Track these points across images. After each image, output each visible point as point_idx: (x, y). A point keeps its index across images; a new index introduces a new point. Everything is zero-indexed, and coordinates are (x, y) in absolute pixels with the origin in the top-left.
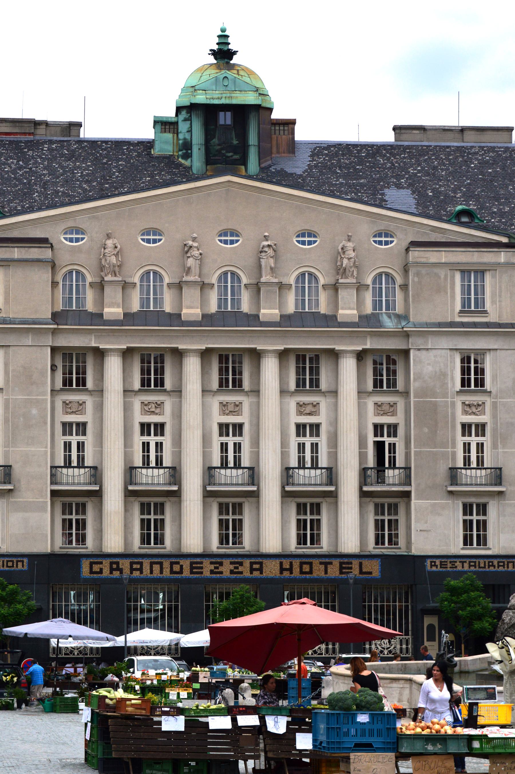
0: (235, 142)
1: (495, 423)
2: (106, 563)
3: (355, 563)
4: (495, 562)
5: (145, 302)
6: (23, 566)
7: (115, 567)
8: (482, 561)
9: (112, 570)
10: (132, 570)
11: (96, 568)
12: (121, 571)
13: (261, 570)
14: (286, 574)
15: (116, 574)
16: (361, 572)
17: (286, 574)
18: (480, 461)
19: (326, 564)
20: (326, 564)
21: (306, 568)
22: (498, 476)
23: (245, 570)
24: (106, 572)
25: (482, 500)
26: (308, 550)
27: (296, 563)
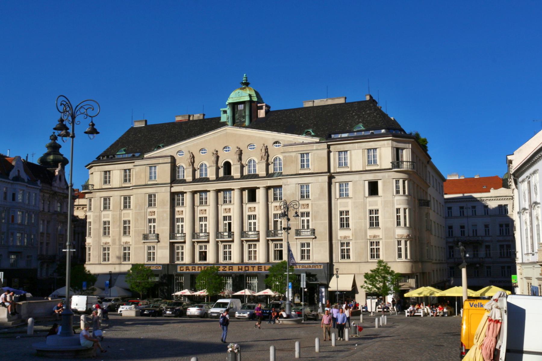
0: (243, 114)
1: (312, 211)
3: (263, 266)
4: (311, 266)
5: (201, 175)
7: (187, 269)
8: (306, 265)
9: (186, 269)
10: (192, 269)
11: (182, 269)
12: (189, 270)
13: (232, 269)
14: (240, 271)
15: (188, 271)
16: (265, 270)
17: (240, 271)
18: (308, 226)
19: (253, 267)
20: (253, 267)
21: (247, 268)
22: (313, 231)
23: (227, 269)
24: (185, 270)
25: (308, 241)
26: (252, 261)
27: (244, 266)
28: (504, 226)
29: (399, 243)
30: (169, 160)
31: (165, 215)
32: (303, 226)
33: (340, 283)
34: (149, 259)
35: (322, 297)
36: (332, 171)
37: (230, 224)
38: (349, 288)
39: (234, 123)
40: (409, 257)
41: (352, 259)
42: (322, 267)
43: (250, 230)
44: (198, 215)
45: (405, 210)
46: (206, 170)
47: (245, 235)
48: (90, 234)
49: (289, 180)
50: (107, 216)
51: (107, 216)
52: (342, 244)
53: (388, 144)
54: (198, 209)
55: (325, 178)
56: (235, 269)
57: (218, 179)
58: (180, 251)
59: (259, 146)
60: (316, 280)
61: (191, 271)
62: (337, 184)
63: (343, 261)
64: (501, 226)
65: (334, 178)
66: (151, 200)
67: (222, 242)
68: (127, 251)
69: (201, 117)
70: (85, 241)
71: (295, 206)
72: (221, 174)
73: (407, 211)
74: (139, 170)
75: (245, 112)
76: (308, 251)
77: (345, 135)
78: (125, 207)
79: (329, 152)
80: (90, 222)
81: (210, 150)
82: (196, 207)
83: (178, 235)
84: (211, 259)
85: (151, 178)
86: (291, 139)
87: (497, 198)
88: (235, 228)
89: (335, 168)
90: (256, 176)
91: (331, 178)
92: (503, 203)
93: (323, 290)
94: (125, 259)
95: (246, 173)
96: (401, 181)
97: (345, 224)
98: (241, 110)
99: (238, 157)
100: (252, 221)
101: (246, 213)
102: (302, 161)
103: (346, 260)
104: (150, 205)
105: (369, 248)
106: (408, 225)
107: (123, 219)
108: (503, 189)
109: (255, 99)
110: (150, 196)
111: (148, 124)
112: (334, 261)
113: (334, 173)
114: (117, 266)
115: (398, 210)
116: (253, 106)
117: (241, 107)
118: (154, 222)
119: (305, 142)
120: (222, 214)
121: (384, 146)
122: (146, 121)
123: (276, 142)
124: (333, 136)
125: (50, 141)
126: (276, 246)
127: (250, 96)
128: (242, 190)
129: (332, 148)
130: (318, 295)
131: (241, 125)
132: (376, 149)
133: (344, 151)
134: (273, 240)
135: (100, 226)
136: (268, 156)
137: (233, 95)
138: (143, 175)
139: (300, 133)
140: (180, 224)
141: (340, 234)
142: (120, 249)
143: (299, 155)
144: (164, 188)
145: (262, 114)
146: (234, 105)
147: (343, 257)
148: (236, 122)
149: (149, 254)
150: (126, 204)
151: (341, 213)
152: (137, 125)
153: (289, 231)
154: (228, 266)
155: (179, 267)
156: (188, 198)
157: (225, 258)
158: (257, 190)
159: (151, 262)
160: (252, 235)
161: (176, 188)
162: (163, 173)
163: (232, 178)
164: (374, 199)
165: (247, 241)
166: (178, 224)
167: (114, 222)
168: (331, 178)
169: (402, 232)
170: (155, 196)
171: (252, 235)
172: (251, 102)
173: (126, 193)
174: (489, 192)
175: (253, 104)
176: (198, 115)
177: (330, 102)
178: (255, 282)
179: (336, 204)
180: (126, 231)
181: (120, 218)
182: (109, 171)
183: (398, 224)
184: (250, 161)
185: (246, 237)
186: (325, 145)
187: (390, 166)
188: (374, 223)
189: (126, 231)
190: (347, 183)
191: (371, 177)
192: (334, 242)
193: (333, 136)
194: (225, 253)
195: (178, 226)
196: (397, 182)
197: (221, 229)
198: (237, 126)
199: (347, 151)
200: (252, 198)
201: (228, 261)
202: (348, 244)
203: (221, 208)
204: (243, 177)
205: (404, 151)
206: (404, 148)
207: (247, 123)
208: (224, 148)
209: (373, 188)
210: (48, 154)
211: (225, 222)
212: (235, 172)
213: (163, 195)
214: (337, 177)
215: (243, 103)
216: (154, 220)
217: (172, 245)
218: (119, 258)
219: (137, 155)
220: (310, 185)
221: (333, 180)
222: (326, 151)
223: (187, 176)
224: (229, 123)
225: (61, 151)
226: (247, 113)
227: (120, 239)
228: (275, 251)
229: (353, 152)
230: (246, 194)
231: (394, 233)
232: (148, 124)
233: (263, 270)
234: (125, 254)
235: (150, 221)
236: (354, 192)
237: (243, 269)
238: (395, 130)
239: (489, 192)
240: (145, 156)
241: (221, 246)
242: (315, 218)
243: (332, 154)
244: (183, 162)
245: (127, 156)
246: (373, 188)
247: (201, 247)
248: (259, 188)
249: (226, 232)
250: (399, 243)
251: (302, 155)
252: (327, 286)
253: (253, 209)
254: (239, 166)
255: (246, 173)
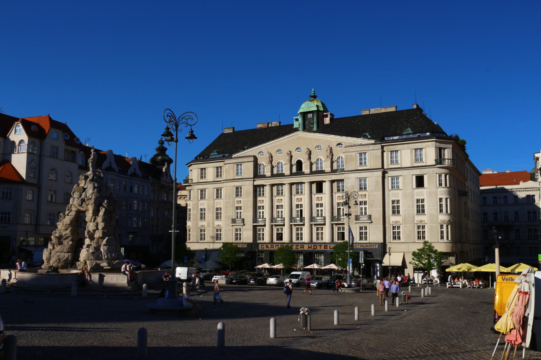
2: (265, 245)
3: (328, 245)
6: (245, 246)
7: (267, 247)
15: (267, 249)
18: (366, 213)
19: (320, 246)
20: (320, 246)
21: (315, 247)
22: (370, 217)
23: (299, 247)
27: (313, 245)
28: (532, 213)
29: (442, 227)
30: (252, 159)
31: (249, 203)
32: (362, 213)
33: (392, 259)
34: (236, 239)
35: (377, 271)
36: (385, 167)
37: (301, 211)
38: (400, 264)
39: (304, 129)
40: (450, 239)
41: (402, 240)
42: (377, 247)
43: (318, 216)
44: (276, 204)
45: (446, 199)
46: (282, 167)
47: (313, 220)
48: (190, 218)
49: (350, 175)
50: (203, 204)
51: (203, 204)
52: (394, 228)
53: (432, 145)
54: (275, 199)
55: (380, 173)
56: (306, 247)
57: (292, 174)
58: (261, 232)
59: (324, 147)
60: (372, 257)
61: (270, 249)
62: (390, 178)
63: (395, 241)
64: (529, 213)
65: (387, 173)
66: (238, 191)
67: (295, 225)
68: (219, 233)
69: (278, 125)
70: (186, 224)
71: (355, 197)
72: (294, 170)
73: (448, 200)
74: (228, 167)
75: (313, 120)
76: (366, 233)
77: (396, 138)
78: (217, 197)
79: (383, 152)
80: (190, 209)
81: (285, 151)
82: (274, 197)
83: (259, 220)
84: (286, 239)
85: (237, 174)
86: (352, 142)
87: (526, 189)
88: (306, 214)
89: (387, 165)
90: (322, 172)
91: (384, 173)
92: (531, 193)
93: (378, 265)
94: (217, 239)
95: (314, 169)
96: (443, 176)
97: (396, 211)
98: (310, 118)
99: (308, 157)
100: (320, 208)
101: (315, 202)
102: (361, 159)
103: (397, 241)
104: (237, 195)
105: (416, 230)
106: (449, 212)
107: (216, 207)
108: (530, 181)
109: (321, 109)
110: (237, 188)
111: (235, 130)
112: (387, 242)
113: (387, 169)
114: (211, 244)
115: (441, 200)
116: (319, 114)
117: (310, 116)
118: (241, 209)
119: (363, 143)
120: (295, 203)
121: (428, 146)
122: (234, 128)
123: (339, 144)
124: (386, 138)
125: (159, 145)
126: (339, 229)
127: (317, 106)
128: (311, 183)
129: (385, 148)
130: (374, 269)
131: (310, 130)
132: (422, 149)
133: (396, 151)
134: (336, 224)
135: (198, 212)
136: (332, 155)
137: (303, 106)
138: (231, 171)
139: (358, 136)
140: (261, 211)
141: (392, 219)
142: (213, 230)
143: (358, 155)
144: (248, 182)
145: (327, 121)
146: (304, 114)
147: (394, 238)
148: (306, 128)
149: (237, 235)
150: (218, 193)
151: (393, 202)
152: (227, 131)
153: (350, 217)
154: (300, 245)
155: (260, 245)
156: (267, 189)
157: (298, 239)
158: (324, 183)
159: (238, 241)
160: (319, 220)
161: (258, 182)
162: (248, 169)
163: (303, 174)
164: (420, 190)
165: (315, 225)
166: (259, 211)
167: (208, 209)
168: (384, 173)
169: (444, 218)
170: (241, 188)
171: (319, 220)
172: (318, 111)
173: (218, 186)
174: (519, 184)
175: (320, 113)
176: (276, 122)
177: (383, 110)
178: (322, 258)
179: (389, 194)
180: (218, 216)
181: (214, 206)
182: (205, 169)
183: (441, 211)
184: (318, 160)
185: (315, 221)
186: (379, 146)
187: (434, 163)
188: (421, 210)
189: (218, 216)
190: (398, 177)
191: (418, 172)
192: (387, 225)
193: (386, 138)
194: (297, 234)
195: (260, 212)
196: (440, 176)
197: (294, 215)
198: (307, 131)
199: (397, 151)
200: (320, 190)
201: (300, 241)
202: (399, 227)
203: (294, 198)
204: (312, 173)
205: (446, 150)
206: (446, 148)
207: (315, 129)
208: (297, 149)
209: (420, 182)
210: (156, 156)
211: (297, 209)
212: (306, 169)
213: (248, 187)
214: (389, 172)
215: (312, 112)
216: (241, 208)
217: (255, 227)
218: (212, 237)
219: (227, 155)
220: (367, 179)
221: (386, 175)
222: (380, 151)
223: (268, 172)
224: (301, 129)
225: (167, 153)
226: (315, 120)
227: (213, 223)
228: (338, 233)
229: (403, 151)
230: (314, 186)
231: (437, 218)
232: (235, 130)
233: (329, 249)
234: (217, 234)
235: (237, 208)
236: (404, 184)
237: (313, 248)
238: (438, 133)
239: (519, 184)
240: (233, 156)
241: (294, 229)
242: (371, 206)
243: (385, 154)
244: (263, 161)
245: (218, 156)
246: (420, 182)
247: (278, 230)
248: (325, 182)
249: (298, 217)
250: (442, 227)
251: (361, 154)
252: (381, 262)
253: (320, 199)
254: (309, 164)
255: (314, 169)
